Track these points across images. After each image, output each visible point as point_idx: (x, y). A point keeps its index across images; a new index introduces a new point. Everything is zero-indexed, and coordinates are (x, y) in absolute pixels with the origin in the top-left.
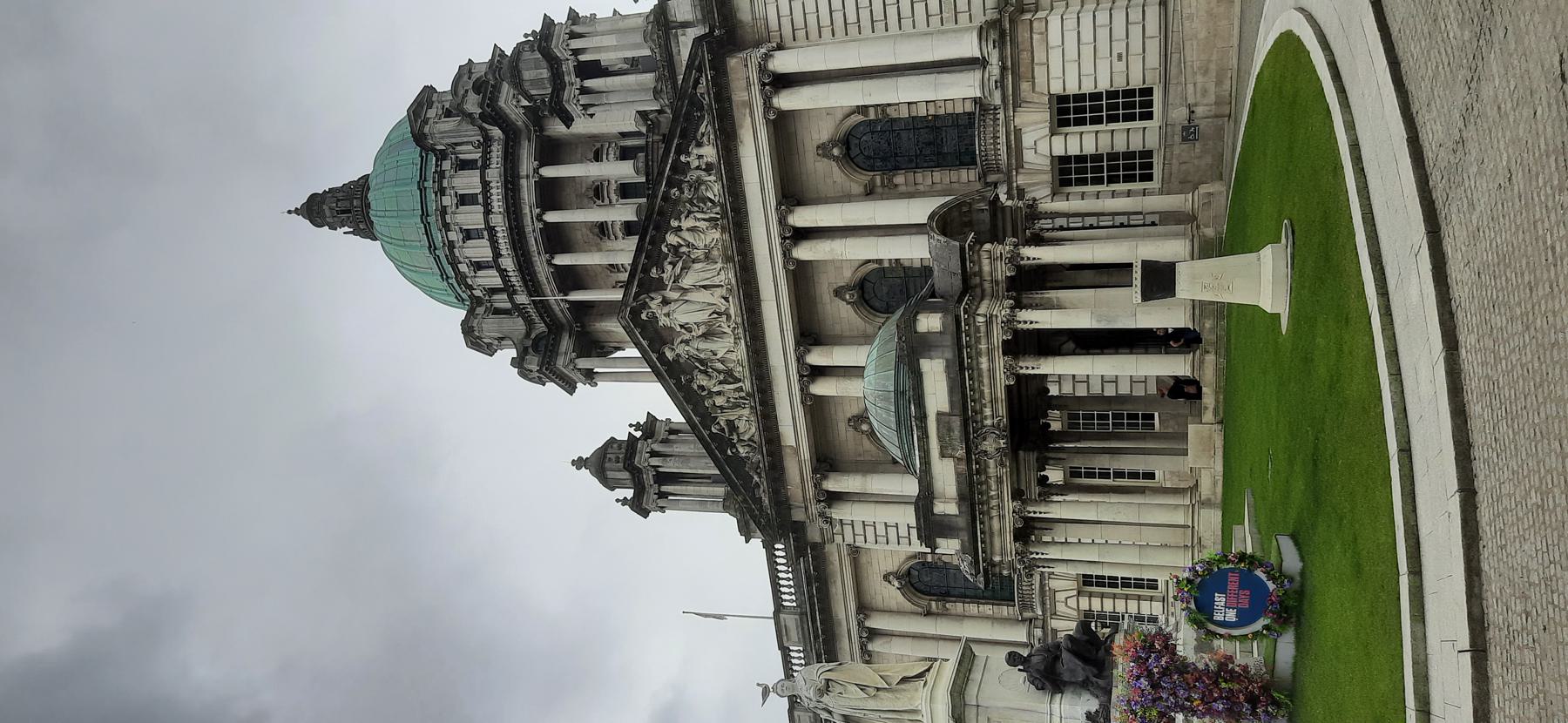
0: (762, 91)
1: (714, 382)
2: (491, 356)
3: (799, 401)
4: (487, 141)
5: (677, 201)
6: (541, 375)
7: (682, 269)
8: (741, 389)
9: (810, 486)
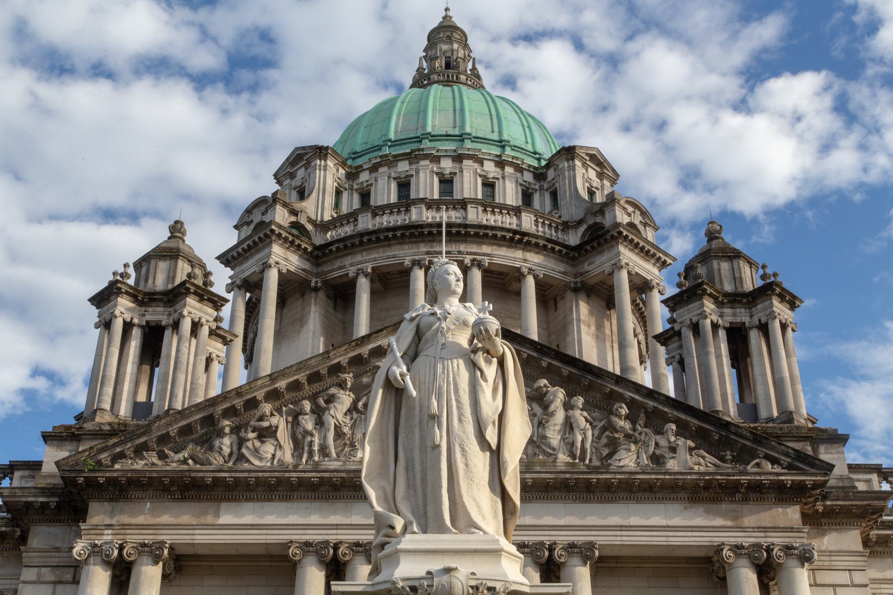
0: (757, 546)
1: (340, 417)
2: (276, 176)
4: (566, 226)
5: (610, 412)
6: (252, 227)
9: (148, 538)
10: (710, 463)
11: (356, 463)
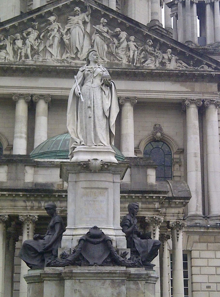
1: (33, 42)
3: (15, 92)
5: (146, 43)
7: (104, 37)
8: (27, 57)
10: (184, 66)
11: (40, 62)
